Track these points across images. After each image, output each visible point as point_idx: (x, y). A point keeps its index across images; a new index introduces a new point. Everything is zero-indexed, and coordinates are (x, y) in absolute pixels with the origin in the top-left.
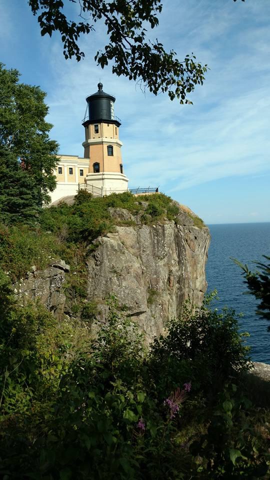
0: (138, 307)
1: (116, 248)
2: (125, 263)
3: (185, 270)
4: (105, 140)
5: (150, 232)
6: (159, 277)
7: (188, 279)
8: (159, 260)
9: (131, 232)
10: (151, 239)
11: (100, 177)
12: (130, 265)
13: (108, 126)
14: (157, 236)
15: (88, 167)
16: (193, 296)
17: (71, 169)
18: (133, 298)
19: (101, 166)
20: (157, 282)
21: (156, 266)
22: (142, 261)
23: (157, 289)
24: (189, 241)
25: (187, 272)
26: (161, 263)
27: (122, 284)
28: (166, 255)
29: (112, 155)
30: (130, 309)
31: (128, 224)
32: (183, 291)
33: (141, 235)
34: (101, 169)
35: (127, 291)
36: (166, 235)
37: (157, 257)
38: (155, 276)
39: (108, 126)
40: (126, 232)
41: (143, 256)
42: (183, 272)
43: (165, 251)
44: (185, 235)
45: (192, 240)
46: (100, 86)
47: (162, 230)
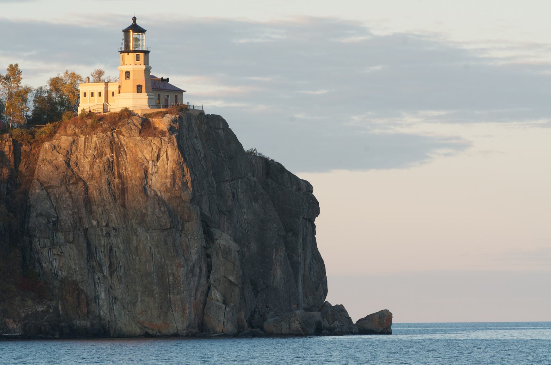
3: (125, 170)
13: (128, 54)
21: (84, 163)
23: (83, 177)
26: (87, 160)
32: (126, 185)
33: (79, 142)
36: (93, 142)
38: (83, 169)
39: (128, 54)
42: (124, 171)
45: (132, 147)
46: (134, 19)
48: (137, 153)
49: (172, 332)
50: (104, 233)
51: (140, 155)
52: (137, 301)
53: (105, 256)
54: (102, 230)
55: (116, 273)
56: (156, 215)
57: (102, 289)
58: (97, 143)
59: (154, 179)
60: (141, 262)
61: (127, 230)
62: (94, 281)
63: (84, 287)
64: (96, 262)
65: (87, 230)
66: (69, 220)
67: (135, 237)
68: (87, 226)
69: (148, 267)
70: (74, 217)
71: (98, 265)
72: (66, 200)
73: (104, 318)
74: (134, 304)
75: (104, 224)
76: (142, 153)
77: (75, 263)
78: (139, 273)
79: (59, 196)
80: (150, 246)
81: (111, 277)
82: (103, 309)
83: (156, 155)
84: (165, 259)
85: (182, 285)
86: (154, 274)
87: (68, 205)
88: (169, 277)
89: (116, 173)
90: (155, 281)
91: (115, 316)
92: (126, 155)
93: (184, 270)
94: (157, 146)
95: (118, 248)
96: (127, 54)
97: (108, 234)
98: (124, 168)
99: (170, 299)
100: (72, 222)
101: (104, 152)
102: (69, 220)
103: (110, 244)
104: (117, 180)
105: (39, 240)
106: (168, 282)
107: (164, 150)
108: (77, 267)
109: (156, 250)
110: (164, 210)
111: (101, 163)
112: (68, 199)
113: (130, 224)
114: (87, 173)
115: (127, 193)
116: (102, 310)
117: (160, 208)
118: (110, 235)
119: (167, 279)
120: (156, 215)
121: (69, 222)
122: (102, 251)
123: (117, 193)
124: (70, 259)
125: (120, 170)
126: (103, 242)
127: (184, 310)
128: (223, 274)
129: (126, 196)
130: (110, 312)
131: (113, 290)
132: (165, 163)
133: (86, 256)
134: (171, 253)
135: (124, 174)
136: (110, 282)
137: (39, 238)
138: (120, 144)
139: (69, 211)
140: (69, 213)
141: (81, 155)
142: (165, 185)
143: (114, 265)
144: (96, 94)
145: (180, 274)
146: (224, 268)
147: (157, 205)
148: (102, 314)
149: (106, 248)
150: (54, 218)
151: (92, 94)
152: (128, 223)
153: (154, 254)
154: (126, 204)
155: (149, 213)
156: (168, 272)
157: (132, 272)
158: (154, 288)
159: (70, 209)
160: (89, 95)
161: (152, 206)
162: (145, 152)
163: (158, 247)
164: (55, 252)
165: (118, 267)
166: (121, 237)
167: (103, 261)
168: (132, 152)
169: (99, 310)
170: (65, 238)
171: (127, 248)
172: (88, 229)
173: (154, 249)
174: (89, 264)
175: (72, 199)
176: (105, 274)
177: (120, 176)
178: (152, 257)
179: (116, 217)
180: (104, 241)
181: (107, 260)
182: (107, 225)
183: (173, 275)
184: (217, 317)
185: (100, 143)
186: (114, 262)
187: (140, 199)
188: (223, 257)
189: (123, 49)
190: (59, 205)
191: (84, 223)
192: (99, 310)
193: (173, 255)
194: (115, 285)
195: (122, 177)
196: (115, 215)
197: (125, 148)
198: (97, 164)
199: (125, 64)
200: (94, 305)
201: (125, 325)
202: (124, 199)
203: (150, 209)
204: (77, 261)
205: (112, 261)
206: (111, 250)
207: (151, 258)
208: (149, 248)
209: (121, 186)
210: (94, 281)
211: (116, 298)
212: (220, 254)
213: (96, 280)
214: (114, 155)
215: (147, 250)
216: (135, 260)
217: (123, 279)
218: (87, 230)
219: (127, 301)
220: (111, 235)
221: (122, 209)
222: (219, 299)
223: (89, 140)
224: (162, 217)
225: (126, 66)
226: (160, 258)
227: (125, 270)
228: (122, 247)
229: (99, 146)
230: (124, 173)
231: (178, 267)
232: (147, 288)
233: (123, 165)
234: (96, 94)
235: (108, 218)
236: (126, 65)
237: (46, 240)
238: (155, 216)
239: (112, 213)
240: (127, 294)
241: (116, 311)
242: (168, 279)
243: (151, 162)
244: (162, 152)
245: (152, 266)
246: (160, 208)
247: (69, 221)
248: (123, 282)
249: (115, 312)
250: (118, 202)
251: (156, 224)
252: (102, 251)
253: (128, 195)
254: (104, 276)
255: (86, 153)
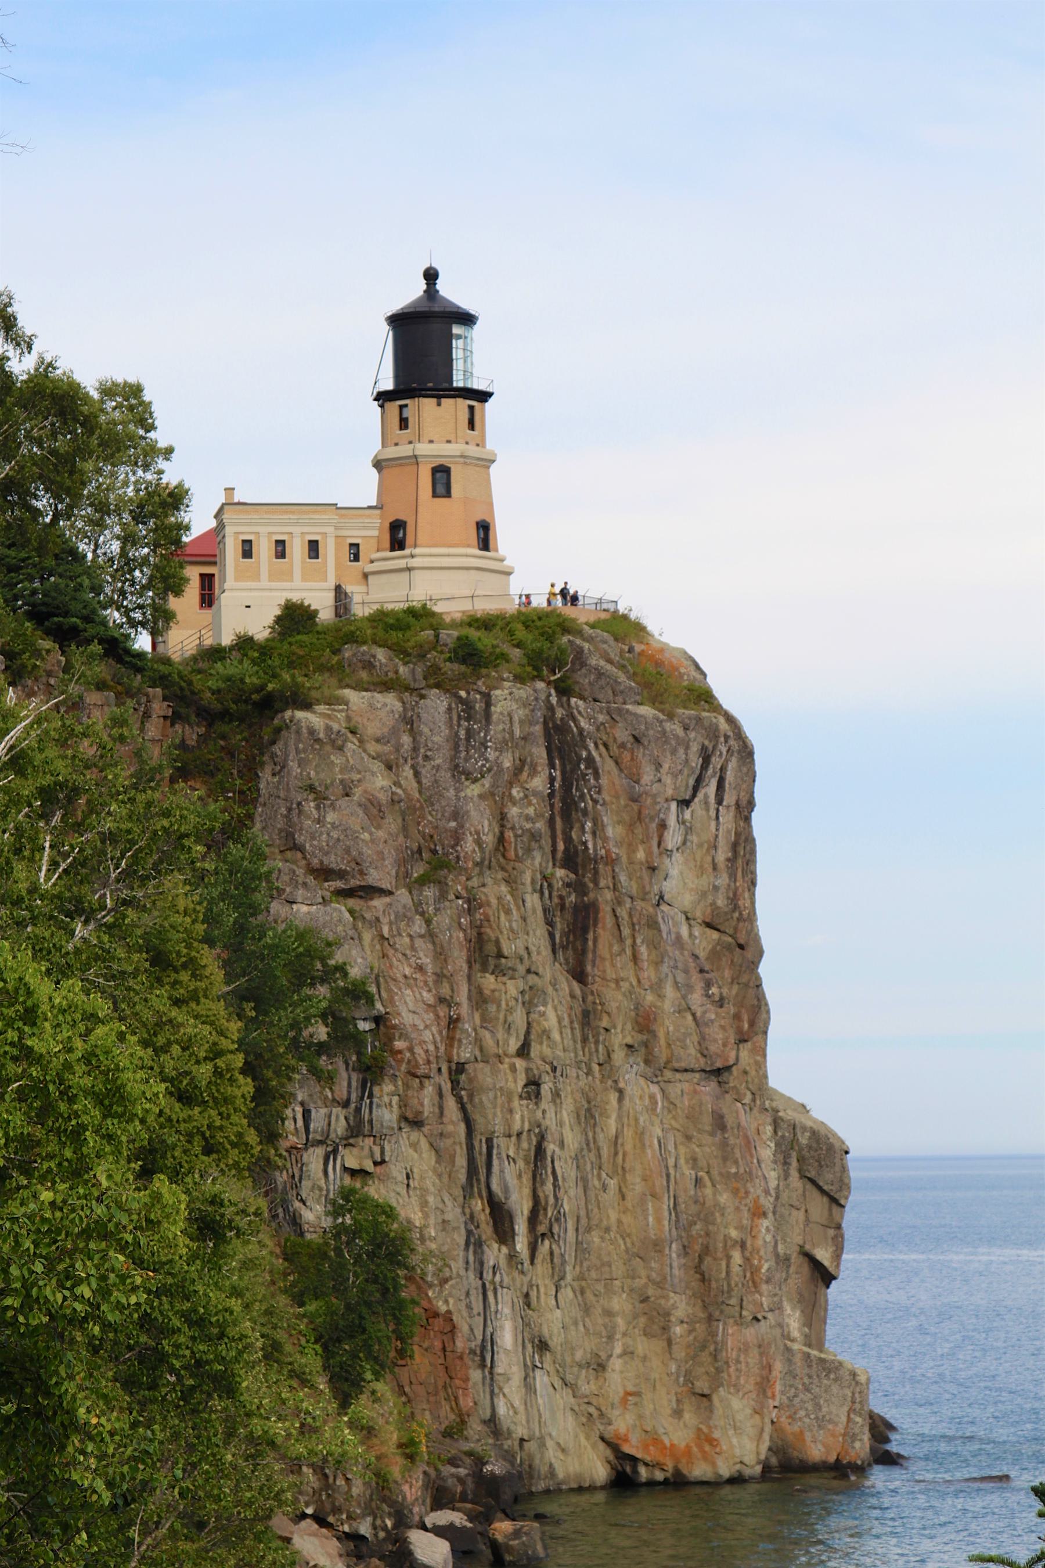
0: (362, 873)
1: (322, 736)
2: (341, 772)
3: (594, 833)
4: (423, 449)
5: (449, 709)
6: (463, 827)
7: (611, 861)
8: (467, 783)
9: (385, 705)
10: (451, 727)
11: (401, 563)
12: (356, 777)
13: (439, 404)
14: (468, 719)
15: (376, 533)
16: (630, 916)
17: (281, 543)
18: (348, 851)
19: (410, 529)
20: (457, 838)
21: (458, 799)
22: (419, 782)
23: (458, 858)
24: (614, 749)
25: (605, 839)
26: (473, 790)
27: (324, 817)
28: (489, 770)
29: (448, 494)
30: (341, 874)
31: (386, 685)
32: (592, 895)
33: (424, 716)
34: (409, 540)
35: (335, 834)
36: (495, 717)
37: (460, 773)
38: (453, 824)
39: (439, 404)
40: (371, 705)
41: (423, 771)
42: (588, 837)
43: (487, 760)
44: (598, 729)
45: (622, 746)
46: (431, 276)
47: (483, 705)
48: (638, 767)
49: (725, 1471)
50: (522, 1080)
51: (647, 778)
52: (611, 1356)
53: (520, 1176)
54: (513, 1069)
55: (547, 1242)
56: (694, 1015)
57: (507, 1311)
58: (516, 718)
59: (674, 872)
60: (623, 1198)
61: (589, 1072)
62: (481, 1278)
63: (451, 1301)
64: (481, 1197)
65: (460, 1068)
66: (426, 1027)
67: (613, 1097)
68: (465, 1053)
69: (651, 1219)
70: (438, 1017)
71: (488, 1211)
72: (413, 948)
73: (508, 1429)
74: (601, 1367)
75: (514, 1045)
76: (658, 766)
77: (424, 1204)
78: (621, 1242)
79: (391, 930)
80: (660, 1134)
81: (532, 1263)
82: (506, 1390)
83: (692, 782)
84: (714, 1186)
85: (764, 1287)
86: (674, 1246)
87: (420, 968)
88: (729, 1258)
89: (561, 846)
90: (676, 1272)
91: (540, 1416)
92: (597, 775)
93: (768, 1230)
94: (704, 748)
95: (562, 1144)
96: (434, 401)
97: (533, 1085)
98: (589, 825)
99: (724, 1343)
100: (438, 1039)
101: (529, 760)
102: (426, 1027)
103: (539, 1126)
104: (560, 873)
105: (307, 1115)
106: (723, 1275)
107: (716, 762)
108: (432, 1221)
109: (682, 1150)
110: (721, 994)
111: (530, 804)
112: (419, 943)
113: (601, 1047)
114: (478, 842)
115: (595, 925)
116: (504, 1395)
117: (708, 984)
118: (538, 1095)
119: (724, 1263)
120: (694, 1015)
121: (427, 1036)
122: (508, 1156)
123: (559, 926)
124: (403, 1191)
125: (574, 835)
126: (518, 1117)
127: (764, 1386)
128: (799, 1240)
129: (590, 936)
130: (526, 1404)
131: (533, 1310)
132: (713, 813)
133: (462, 1176)
134: (736, 1162)
135: (587, 848)
136: (526, 1279)
137: (302, 1104)
138: (575, 729)
139: (425, 994)
140: (424, 1002)
141: (438, 768)
142: (710, 899)
143: (545, 1209)
144: (297, 550)
145: (760, 1242)
146: (801, 1215)
147: (695, 977)
148: (502, 1410)
149: (525, 1145)
150: (364, 1019)
151: (281, 549)
152: (597, 1042)
153: (676, 1166)
154: (589, 968)
155: (668, 1006)
156: (726, 1238)
157: (596, 1240)
158: (672, 1301)
159: (426, 982)
160: (264, 550)
161: (679, 979)
162: (666, 766)
163: (688, 1138)
164: (352, 1163)
165: (557, 1220)
166: (570, 1100)
167: (514, 1197)
168: (617, 763)
169: (492, 1394)
170: (403, 1104)
171: (588, 1145)
172: (466, 1066)
173: (676, 1148)
174: (467, 1211)
175: (434, 943)
176: (518, 1247)
177: (573, 859)
178: (668, 1181)
179: (560, 1020)
180: (522, 1116)
181: (527, 1191)
182: (523, 1051)
183: (743, 1245)
184: (810, 1406)
185: (521, 722)
186: (546, 1197)
187: (643, 950)
188: (803, 1176)
189: (388, 384)
190: (391, 966)
191: (460, 1041)
192: (492, 1393)
193: (742, 1171)
194: (542, 1290)
195: (579, 860)
196: (555, 1009)
197: (592, 746)
198: (514, 804)
199: (425, 438)
200: (476, 1375)
201: (563, 1450)
202: (584, 952)
203: (669, 991)
204: (431, 1199)
205: (541, 1194)
206: (540, 1151)
207: (665, 1183)
208: (656, 1142)
209: (573, 898)
210: (481, 1278)
211: (543, 1346)
212: (794, 1164)
213: (488, 1276)
214: (557, 774)
215: (649, 1151)
216: (605, 1188)
217: (568, 1268)
218: (460, 1068)
219: (579, 1355)
220: (543, 1092)
221: (575, 984)
222: (796, 1334)
223: (472, 708)
224: (712, 1021)
225: (431, 445)
226: (698, 1182)
227: (577, 1230)
228: (572, 1139)
229: (517, 733)
230: (590, 845)
231: (754, 1215)
232: (645, 1300)
233: (585, 812)
234: (297, 550)
235: (529, 1023)
236: (431, 442)
237: (334, 1110)
238: (690, 1018)
239: (545, 1005)
240: (581, 1328)
241: (541, 1396)
242: (728, 1266)
243: (674, 806)
244: (710, 771)
245: (666, 1214)
246: (708, 984)
247: (427, 1033)
248: (569, 1277)
249: (540, 1401)
250: (560, 954)
251: (692, 1051)
252: (508, 1156)
253: (600, 931)
254: (512, 1256)
255: (466, 760)
